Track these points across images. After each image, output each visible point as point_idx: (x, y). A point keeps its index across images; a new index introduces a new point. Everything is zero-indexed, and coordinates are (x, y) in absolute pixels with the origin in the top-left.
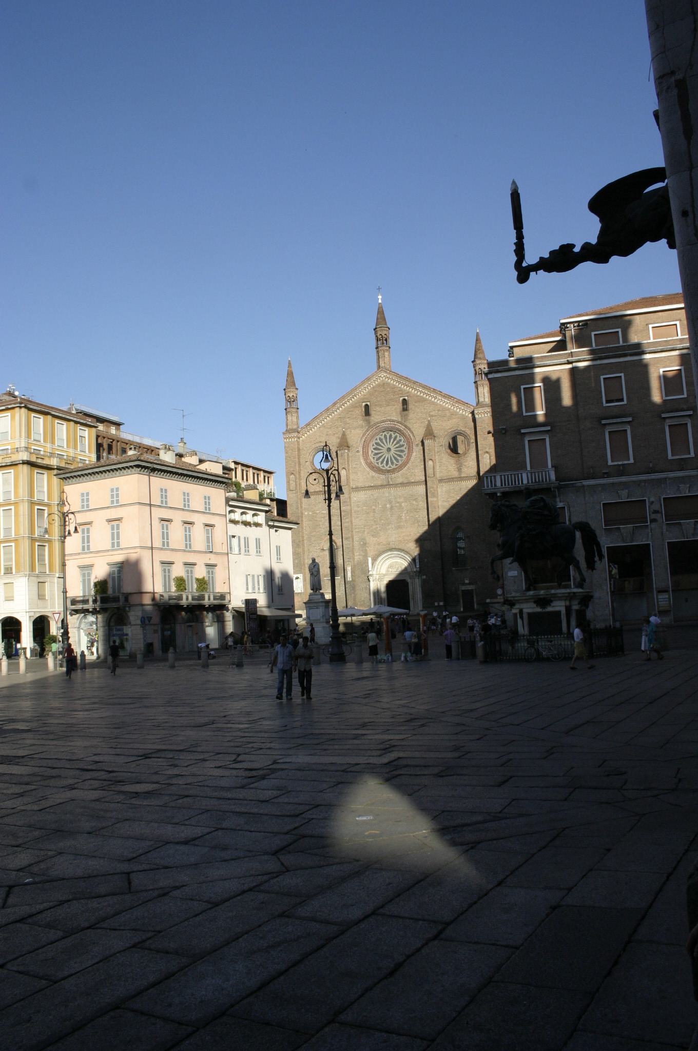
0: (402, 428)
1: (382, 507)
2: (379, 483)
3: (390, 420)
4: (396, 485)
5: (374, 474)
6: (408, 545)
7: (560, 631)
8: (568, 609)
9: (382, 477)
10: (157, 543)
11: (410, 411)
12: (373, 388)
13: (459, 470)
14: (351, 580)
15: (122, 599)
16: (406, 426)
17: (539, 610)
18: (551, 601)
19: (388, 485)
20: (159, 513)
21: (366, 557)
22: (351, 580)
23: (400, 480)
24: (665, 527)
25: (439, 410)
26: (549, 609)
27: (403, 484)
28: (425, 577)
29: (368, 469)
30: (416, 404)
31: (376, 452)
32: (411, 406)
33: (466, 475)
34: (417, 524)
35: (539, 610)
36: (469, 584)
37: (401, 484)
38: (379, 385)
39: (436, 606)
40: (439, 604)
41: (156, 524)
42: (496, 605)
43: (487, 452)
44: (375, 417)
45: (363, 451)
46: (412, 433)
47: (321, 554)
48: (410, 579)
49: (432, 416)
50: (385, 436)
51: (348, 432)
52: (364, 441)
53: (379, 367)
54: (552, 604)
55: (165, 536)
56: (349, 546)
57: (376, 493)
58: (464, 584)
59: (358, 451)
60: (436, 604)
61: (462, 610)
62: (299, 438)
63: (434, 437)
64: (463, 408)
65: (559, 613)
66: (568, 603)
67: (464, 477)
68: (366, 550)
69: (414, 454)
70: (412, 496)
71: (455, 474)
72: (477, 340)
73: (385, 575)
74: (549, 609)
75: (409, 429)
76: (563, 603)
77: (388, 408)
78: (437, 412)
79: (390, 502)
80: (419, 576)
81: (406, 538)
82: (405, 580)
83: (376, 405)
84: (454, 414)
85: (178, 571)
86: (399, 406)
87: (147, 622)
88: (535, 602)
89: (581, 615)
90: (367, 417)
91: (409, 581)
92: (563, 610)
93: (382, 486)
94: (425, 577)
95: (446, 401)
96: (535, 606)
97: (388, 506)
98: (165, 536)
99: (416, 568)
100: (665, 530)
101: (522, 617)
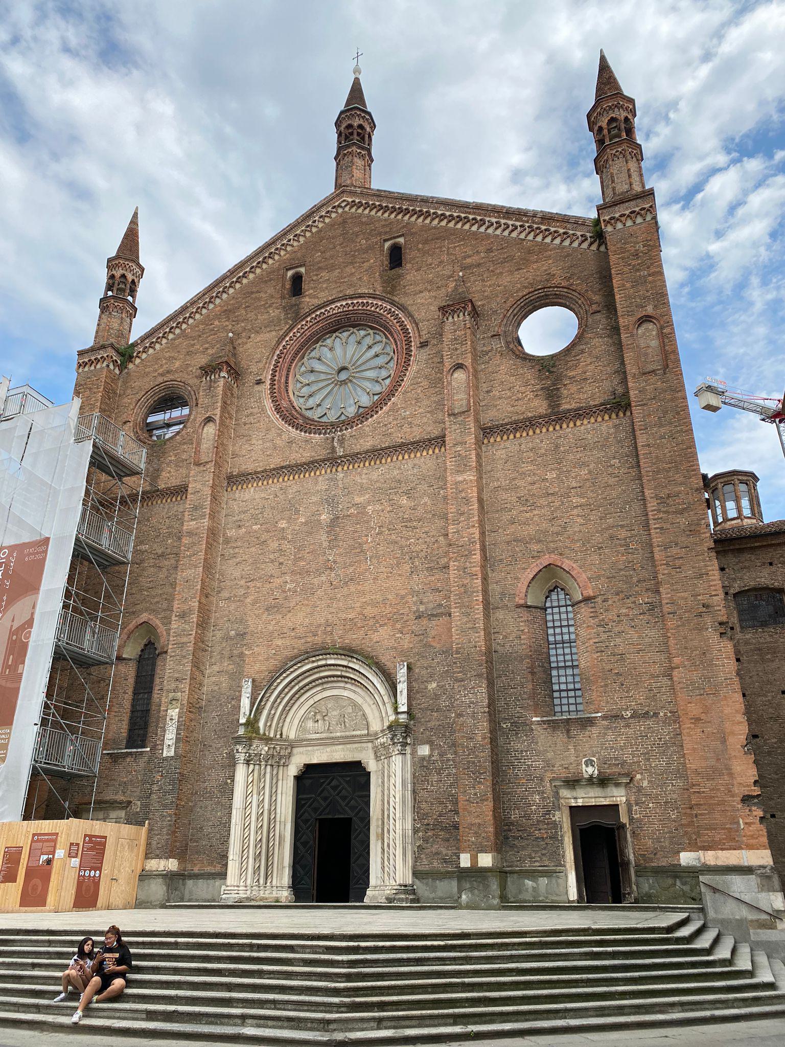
0: (381, 307)
1: (306, 523)
2: (306, 455)
4: (354, 458)
5: (294, 432)
6: (375, 637)
9: (317, 438)
11: (409, 266)
12: (320, 231)
13: (552, 395)
14: (172, 753)
16: (393, 303)
19: (333, 461)
21: (236, 678)
22: (172, 753)
23: (367, 443)
25: (490, 250)
27: (377, 454)
28: (424, 750)
29: (281, 423)
30: (427, 247)
33: (574, 406)
34: (407, 567)
36: (603, 781)
37: (367, 452)
38: (332, 225)
39: (465, 870)
40: (474, 859)
42: (739, 885)
45: (273, 380)
46: (410, 315)
48: (377, 758)
49: (470, 267)
52: (279, 357)
56: (185, 640)
57: (293, 485)
58: (573, 783)
59: (259, 382)
60: (465, 861)
61: (573, 894)
64: (562, 231)
67: (569, 411)
68: (241, 655)
69: (413, 368)
70: (399, 481)
75: (402, 308)
77: (349, 270)
78: (482, 255)
79: (331, 502)
80: (404, 745)
81: (369, 611)
82: (359, 763)
83: (320, 268)
86: (377, 260)
91: (372, 766)
93: (311, 465)
94: (424, 750)
95: (510, 223)
97: (323, 517)
99: (397, 713)
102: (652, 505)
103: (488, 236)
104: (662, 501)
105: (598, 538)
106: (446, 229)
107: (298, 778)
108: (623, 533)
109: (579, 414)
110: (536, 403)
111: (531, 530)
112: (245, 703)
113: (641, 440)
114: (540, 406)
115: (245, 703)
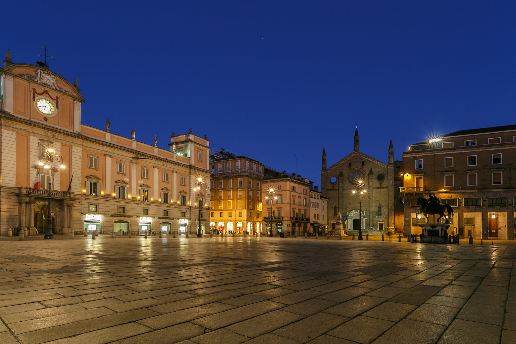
3: (358, 168)
7: (438, 236)
8: (442, 229)
10: (292, 203)
13: (381, 185)
15: (281, 218)
17: (432, 229)
18: (436, 227)
20: (293, 193)
24: (463, 208)
26: (435, 229)
31: (352, 178)
32: (365, 164)
35: (432, 229)
41: (292, 197)
43: (391, 180)
44: (353, 166)
47: (332, 209)
49: (373, 167)
50: (356, 173)
51: (343, 171)
53: (355, 150)
54: (437, 228)
55: (294, 201)
62: (326, 172)
63: (373, 174)
65: (438, 230)
66: (442, 228)
71: (379, 186)
72: (391, 142)
73: (352, 217)
74: (435, 229)
76: (440, 227)
84: (381, 167)
85: (297, 211)
86: (361, 164)
87: (289, 225)
88: (430, 227)
89: (446, 231)
90: (350, 167)
92: (440, 230)
96: (430, 227)
98: (294, 201)
100: (463, 209)
101: (425, 231)
102: (389, 199)
103: (374, 163)
104: (390, 199)
105: (384, 201)
106: (369, 161)
107: (353, 220)
108: (386, 201)
109: (383, 188)
110: (379, 186)
111: (378, 199)
112: (348, 213)
113: (389, 193)
114: (379, 186)
115: (348, 213)
